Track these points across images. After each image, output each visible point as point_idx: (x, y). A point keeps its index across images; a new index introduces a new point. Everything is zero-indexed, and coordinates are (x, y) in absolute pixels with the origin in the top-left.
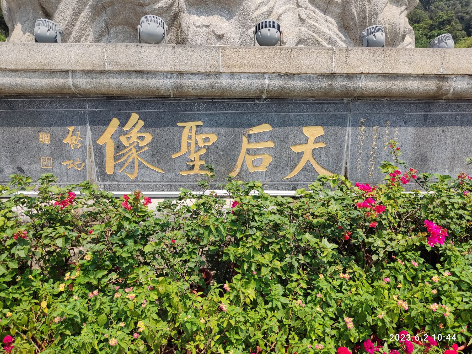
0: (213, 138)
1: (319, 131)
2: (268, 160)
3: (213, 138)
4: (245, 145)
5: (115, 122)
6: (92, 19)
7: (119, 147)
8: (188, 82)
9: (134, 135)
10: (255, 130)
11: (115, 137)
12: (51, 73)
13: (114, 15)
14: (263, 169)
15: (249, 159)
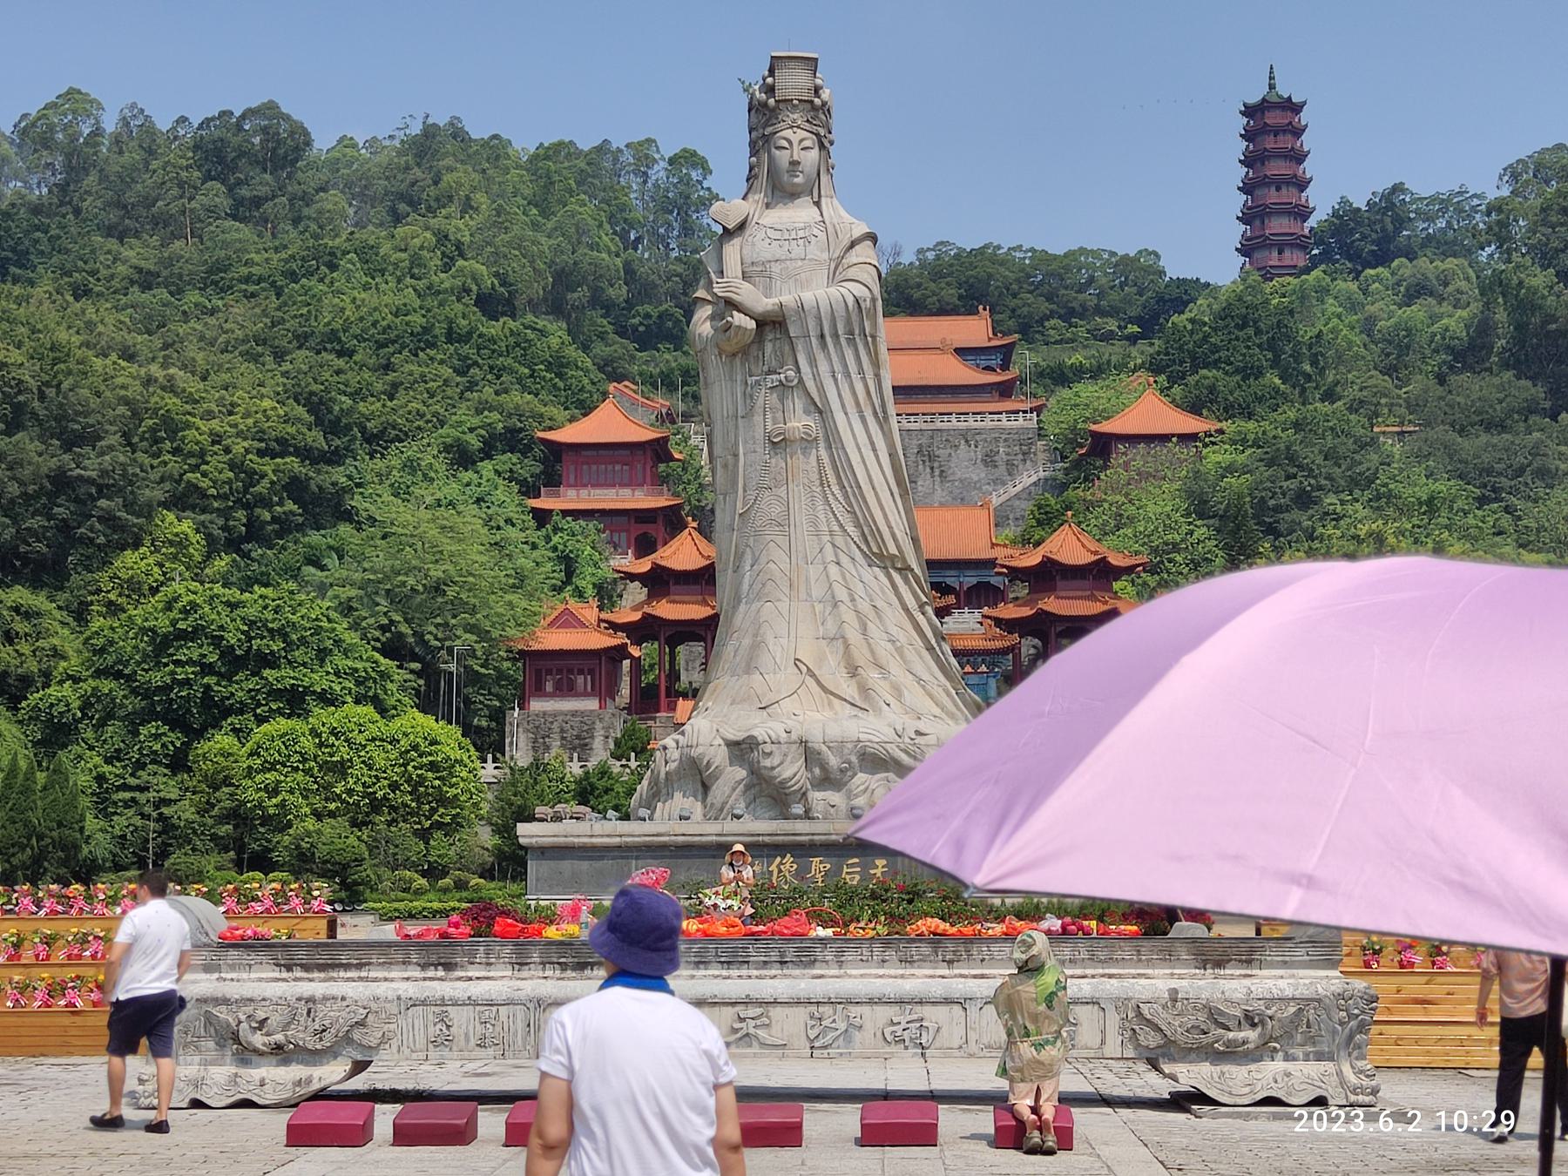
0: (828, 866)
1: (884, 862)
2: (858, 877)
3: (828, 866)
4: (845, 870)
5: (779, 859)
6: (745, 792)
7: (780, 871)
8: (816, 838)
9: (788, 865)
10: (850, 862)
11: (778, 866)
12: (752, 835)
13: (761, 791)
14: (855, 883)
15: (848, 877)
